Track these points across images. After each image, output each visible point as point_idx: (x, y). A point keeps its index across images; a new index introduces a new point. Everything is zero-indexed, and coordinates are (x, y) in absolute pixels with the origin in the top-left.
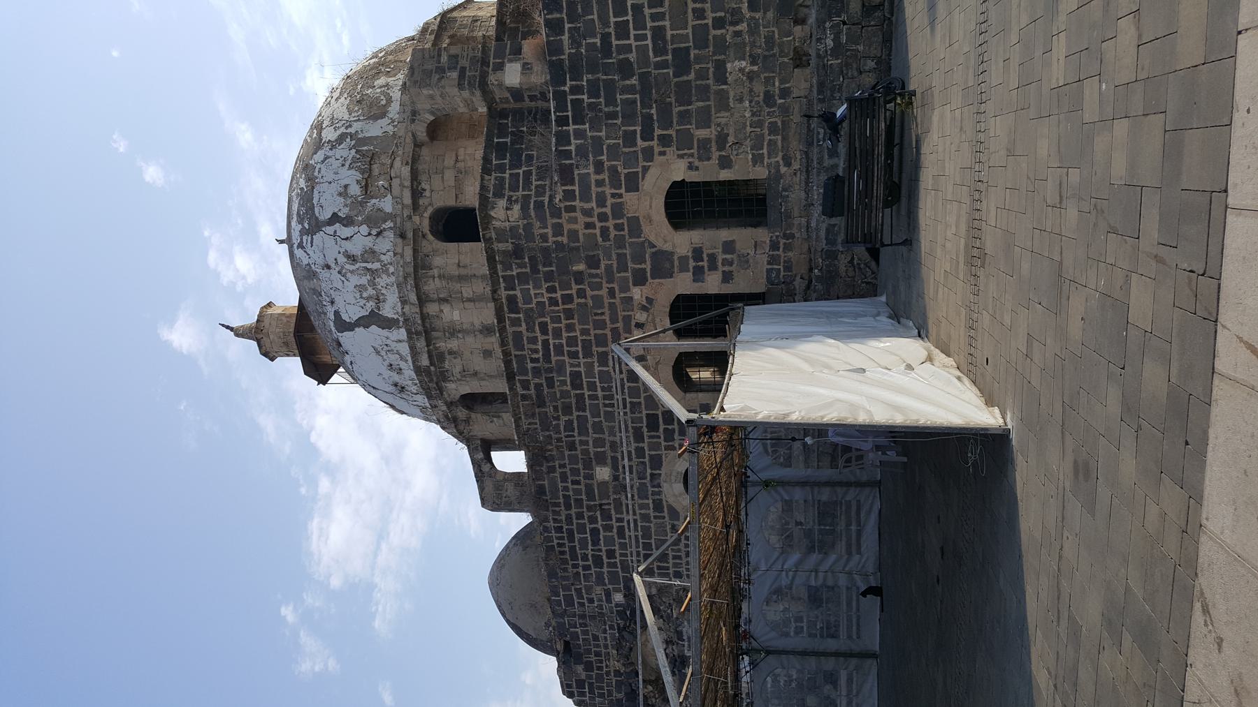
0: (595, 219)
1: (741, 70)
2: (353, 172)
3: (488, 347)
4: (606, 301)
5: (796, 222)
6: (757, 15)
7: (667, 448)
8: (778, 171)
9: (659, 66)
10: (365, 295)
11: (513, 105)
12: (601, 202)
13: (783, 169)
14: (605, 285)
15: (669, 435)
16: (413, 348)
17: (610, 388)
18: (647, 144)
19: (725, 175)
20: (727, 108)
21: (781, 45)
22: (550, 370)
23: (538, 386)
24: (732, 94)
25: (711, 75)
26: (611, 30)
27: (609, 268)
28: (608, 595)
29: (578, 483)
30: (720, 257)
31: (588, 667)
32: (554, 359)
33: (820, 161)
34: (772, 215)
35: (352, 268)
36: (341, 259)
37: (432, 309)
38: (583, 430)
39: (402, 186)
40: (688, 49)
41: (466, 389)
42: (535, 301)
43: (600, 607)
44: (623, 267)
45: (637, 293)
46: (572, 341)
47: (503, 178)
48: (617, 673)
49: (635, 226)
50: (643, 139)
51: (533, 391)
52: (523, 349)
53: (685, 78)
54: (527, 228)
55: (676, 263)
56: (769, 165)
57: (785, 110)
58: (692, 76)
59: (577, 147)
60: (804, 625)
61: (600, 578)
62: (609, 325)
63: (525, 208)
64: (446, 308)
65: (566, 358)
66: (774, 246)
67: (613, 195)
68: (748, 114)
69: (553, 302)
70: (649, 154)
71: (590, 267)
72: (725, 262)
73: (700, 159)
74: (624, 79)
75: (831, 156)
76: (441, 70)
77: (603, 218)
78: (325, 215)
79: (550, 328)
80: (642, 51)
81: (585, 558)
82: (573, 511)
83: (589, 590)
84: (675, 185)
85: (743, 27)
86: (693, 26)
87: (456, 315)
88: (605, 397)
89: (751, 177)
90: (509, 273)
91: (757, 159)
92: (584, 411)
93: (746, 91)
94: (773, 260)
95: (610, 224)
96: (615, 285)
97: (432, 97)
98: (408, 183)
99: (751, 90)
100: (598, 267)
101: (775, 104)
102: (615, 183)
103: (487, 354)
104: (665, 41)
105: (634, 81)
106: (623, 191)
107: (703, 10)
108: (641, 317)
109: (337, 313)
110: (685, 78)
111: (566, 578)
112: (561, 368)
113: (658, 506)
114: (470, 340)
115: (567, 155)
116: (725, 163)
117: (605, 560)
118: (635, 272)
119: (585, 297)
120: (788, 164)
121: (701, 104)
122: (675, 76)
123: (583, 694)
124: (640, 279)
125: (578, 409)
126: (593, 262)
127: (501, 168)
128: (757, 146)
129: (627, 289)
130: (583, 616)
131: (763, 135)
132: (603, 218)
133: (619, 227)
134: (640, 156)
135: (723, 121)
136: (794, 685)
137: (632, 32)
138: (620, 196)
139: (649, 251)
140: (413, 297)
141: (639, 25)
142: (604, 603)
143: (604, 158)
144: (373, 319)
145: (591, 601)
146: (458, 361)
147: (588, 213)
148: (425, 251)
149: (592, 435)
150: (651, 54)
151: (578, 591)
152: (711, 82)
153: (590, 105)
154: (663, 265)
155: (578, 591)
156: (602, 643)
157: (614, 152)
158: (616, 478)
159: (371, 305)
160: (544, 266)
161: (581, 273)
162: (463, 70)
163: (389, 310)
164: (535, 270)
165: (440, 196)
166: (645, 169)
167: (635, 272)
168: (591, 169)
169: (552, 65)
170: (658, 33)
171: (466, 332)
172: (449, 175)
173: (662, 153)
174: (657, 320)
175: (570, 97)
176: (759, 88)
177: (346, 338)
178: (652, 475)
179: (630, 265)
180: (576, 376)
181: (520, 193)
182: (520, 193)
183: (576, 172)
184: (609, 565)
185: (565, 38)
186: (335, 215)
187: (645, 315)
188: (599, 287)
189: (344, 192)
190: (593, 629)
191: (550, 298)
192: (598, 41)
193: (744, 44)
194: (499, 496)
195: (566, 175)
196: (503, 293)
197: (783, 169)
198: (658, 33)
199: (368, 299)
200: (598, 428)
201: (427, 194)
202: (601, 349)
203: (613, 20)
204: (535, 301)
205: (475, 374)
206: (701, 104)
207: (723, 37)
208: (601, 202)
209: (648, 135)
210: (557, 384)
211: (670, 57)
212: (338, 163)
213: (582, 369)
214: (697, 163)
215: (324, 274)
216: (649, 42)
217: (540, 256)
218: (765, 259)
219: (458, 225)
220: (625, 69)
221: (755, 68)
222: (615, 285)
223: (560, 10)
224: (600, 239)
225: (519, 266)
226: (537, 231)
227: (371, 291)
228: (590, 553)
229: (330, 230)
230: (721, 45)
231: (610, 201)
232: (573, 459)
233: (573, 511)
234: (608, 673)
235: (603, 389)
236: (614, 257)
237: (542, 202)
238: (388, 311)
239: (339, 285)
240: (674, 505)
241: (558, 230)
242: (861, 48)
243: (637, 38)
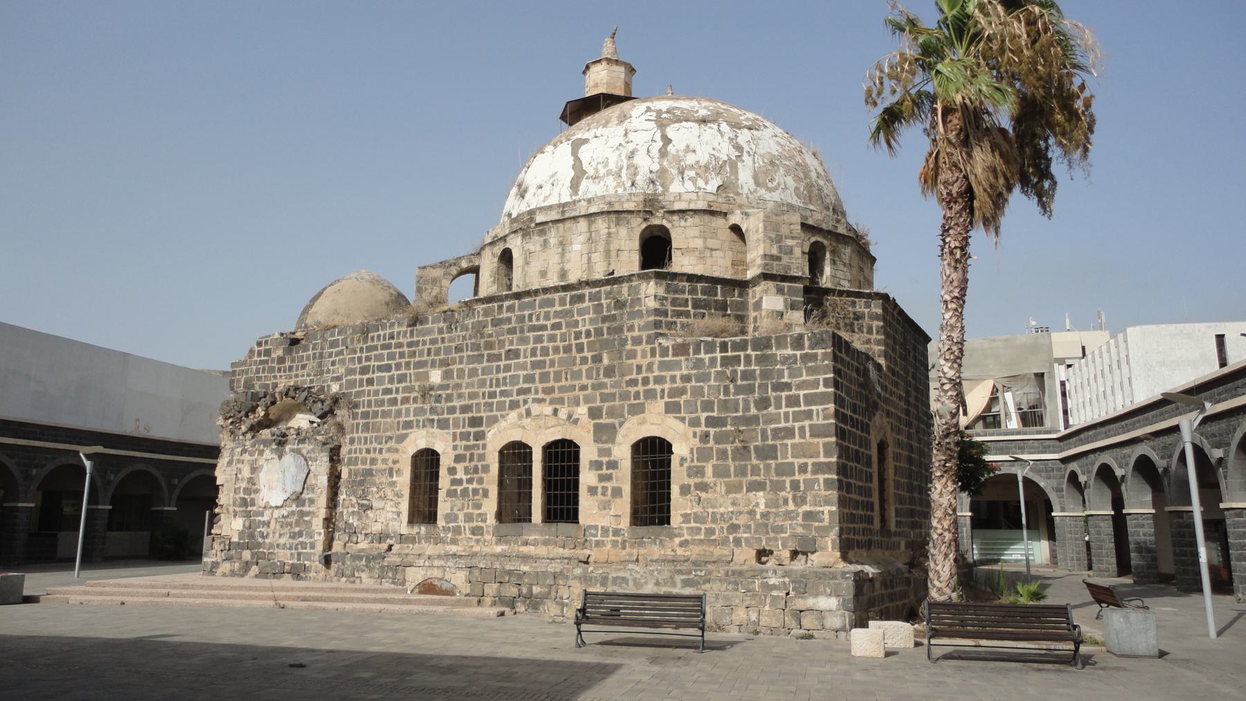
0: (644, 375)
1: (757, 504)
2: (707, 157)
3: (549, 275)
4: (577, 383)
5: (635, 551)
6: (800, 519)
7: (454, 435)
8: (676, 536)
9: (764, 432)
10: (600, 167)
11: (751, 301)
12: (659, 380)
13: (677, 540)
14: (590, 382)
15: (465, 436)
16: (550, 208)
17: (505, 384)
18: (703, 421)
20: (728, 492)
21: (776, 539)
22: (522, 331)
23: (509, 320)
24: (738, 496)
25: (754, 478)
26: (793, 392)
27: (603, 385)
28: (338, 379)
29: (429, 353)
30: (609, 485)
31: (281, 360)
32: (531, 335)
33: (680, 572)
34: (642, 530)
35: (623, 156)
36: (631, 147)
37: (583, 224)
38: (472, 360)
39: (690, 201)
40: (776, 458)
41: (516, 254)
42: (579, 319)
43: (328, 371)
44: (605, 398)
45: (582, 410)
46: (545, 351)
47: (684, 292)
48: (275, 386)
49: (637, 410)
50: (707, 418)
51: (505, 315)
52: (540, 307)
53: (753, 455)
54: (639, 314)
55: (606, 446)
56: (681, 528)
57: (725, 542)
58: (754, 461)
59: (702, 360)
60: (308, 550)
61: (351, 372)
62: (557, 385)
63: (657, 312)
64: (582, 238)
65: (531, 346)
66: (617, 532)
67: (663, 391)
68: (722, 510)
69: (578, 335)
70: (695, 423)
71: (606, 369)
72: (605, 489)
73: (689, 468)
74: (756, 402)
75: (683, 581)
76: (779, 239)
77: (646, 381)
78: (671, 132)
79: (557, 332)
80: (776, 419)
81: (368, 359)
82: (406, 349)
83: (342, 362)
84: (670, 446)
85: (791, 506)
86: (793, 464)
87: (577, 247)
88: (498, 380)
89: (672, 512)
90: (603, 296)
91: (686, 517)
92: (488, 361)
93: (741, 508)
94: (605, 531)
95: (640, 388)
96: (590, 391)
97: (757, 231)
98: (692, 206)
99: (741, 513)
100: (606, 375)
101: (729, 533)
103: (543, 274)
104: (785, 437)
105: (753, 411)
106: (666, 399)
107: (805, 472)
108: (563, 413)
109: (586, 141)
110: (753, 455)
111: (352, 340)
112: (524, 341)
113: (408, 425)
114: (556, 258)
115: (697, 351)
116: (685, 490)
117: (365, 377)
118: (600, 409)
119: (581, 364)
120: (681, 545)
121: (732, 469)
122: (756, 448)
123: (259, 355)
124: (594, 413)
125: (489, 355)
126: (609, 372)
127: (693, 291)
128: (699, 518)
129: (586, 402)
130: (321, 355)
131: (704, 523)
132: (646, 381)
133: (637, 395)
134: (694, 415)
135: (718, 489)
136: (260, 540)
137: (791, 410)
138: (662, 397)
139: (616, 422)
140: (593, 209)
141: (798, 417)
142: (331, 375)
143: (693, 383)
144: (579, 174)
145: (333, 363)
146: (538, 248)
147: (650, 367)
148: (633, 220)
149: (467, 367)
150: (773, 426)
151: (341, 353)
152: (749, 478)
153: (736, 371)
154: (605, 433)
155: (341, 353)
156: (300, 372)
157: (698, 392)
158: (432, 388)
159: (590, 171)
160: (608, 328)
161: (601, 360)
162: (779, 259)
163: (588, 188)
164: (605, 319)
165: (683, 235)
166: (683, 420)
167: (600, 409)
168: (685, 372)
169: (769, 339)
170: (789, 433)
171: (563, 255)
172: (699, 243)
173: (695, 435)
174: (559, 428)
175: (742, 354)
176: (741, 520)
177: (565, 148)
178: (433, 420)
179: (606, 405)
180: (516, 354)
181: (670, 308)
182: (670, 308)
183: (683, 358)
184: (361, 380)
185: (789, 352)
186: (670, 141)
187: (565, 417)
188: (589, 377)
189: (689, 150)
190: (311, 364)
191: (580, 333)
192: (785, 380)
193: (777, 507)
194: (426, 282)
195: (681, 349)
196: (587, 291)
197: (677, 540)
198: (789, 433)
199: (596, 170)
200: (473, 373)
201: (683, 223)
202: (537, 377)
203: (802, 393)
204: (579, 319)
205: (527, 263)
206: (732, 469)
207: (783, 489)
208: (659, 380)
209: (711, 422)
210: (510, 337)
211: (770, 442)
212: (716, 145)
213: (522, 360)
214: (686, 465)
215: (620, 130)
216: (783, 425)
217: (615, 324)
218: (606, 524)
219: (656, 249)
220: (763, 403)
221: (758, 517)
222: (590, 391)
223: (811, 347)
224: (627, 378)
225: (609, 305)
226: (637, 322)
227: (602, 171)
228: (372, 363)
229: (658, 136)
230: (777, 487)
231: (658, 387)
232: (448, 351)
233: (406, 349)
234: (275, 377)
235: (505, 378)
236: (613, 391)
237: (660, 327)
238: (585, 184)
239: (609, 144)
240: (408, 440)
241: (637, 341)
242: (767, 608)
243: (786, 414)
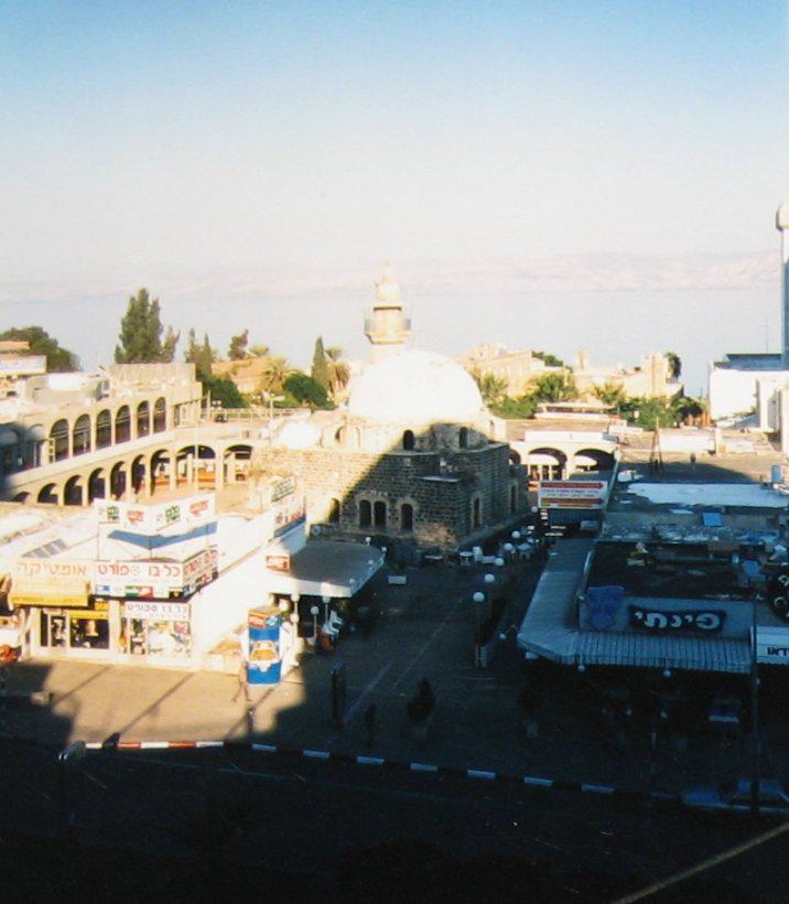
19: (414, 520)
45: (386, 494)
49: (402, 496)
102: (414, 492)
124: (390, 495)
